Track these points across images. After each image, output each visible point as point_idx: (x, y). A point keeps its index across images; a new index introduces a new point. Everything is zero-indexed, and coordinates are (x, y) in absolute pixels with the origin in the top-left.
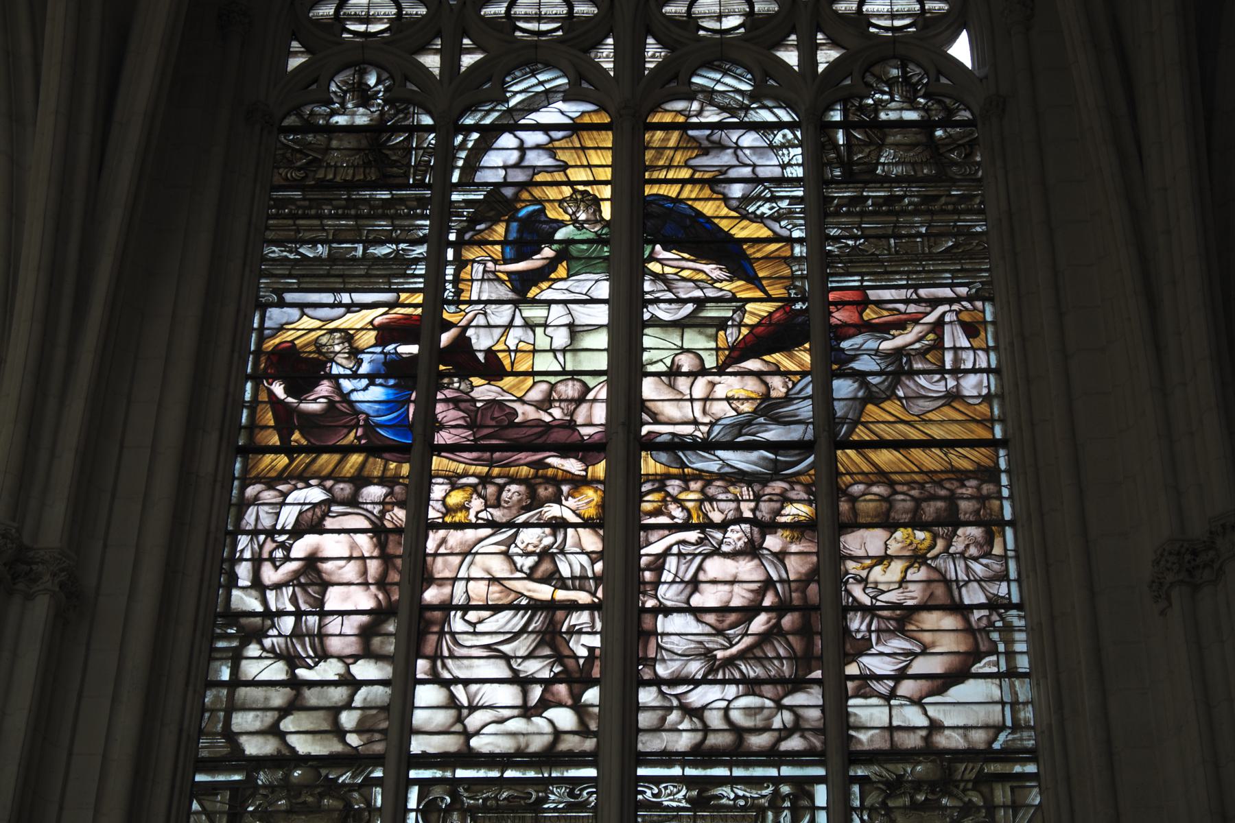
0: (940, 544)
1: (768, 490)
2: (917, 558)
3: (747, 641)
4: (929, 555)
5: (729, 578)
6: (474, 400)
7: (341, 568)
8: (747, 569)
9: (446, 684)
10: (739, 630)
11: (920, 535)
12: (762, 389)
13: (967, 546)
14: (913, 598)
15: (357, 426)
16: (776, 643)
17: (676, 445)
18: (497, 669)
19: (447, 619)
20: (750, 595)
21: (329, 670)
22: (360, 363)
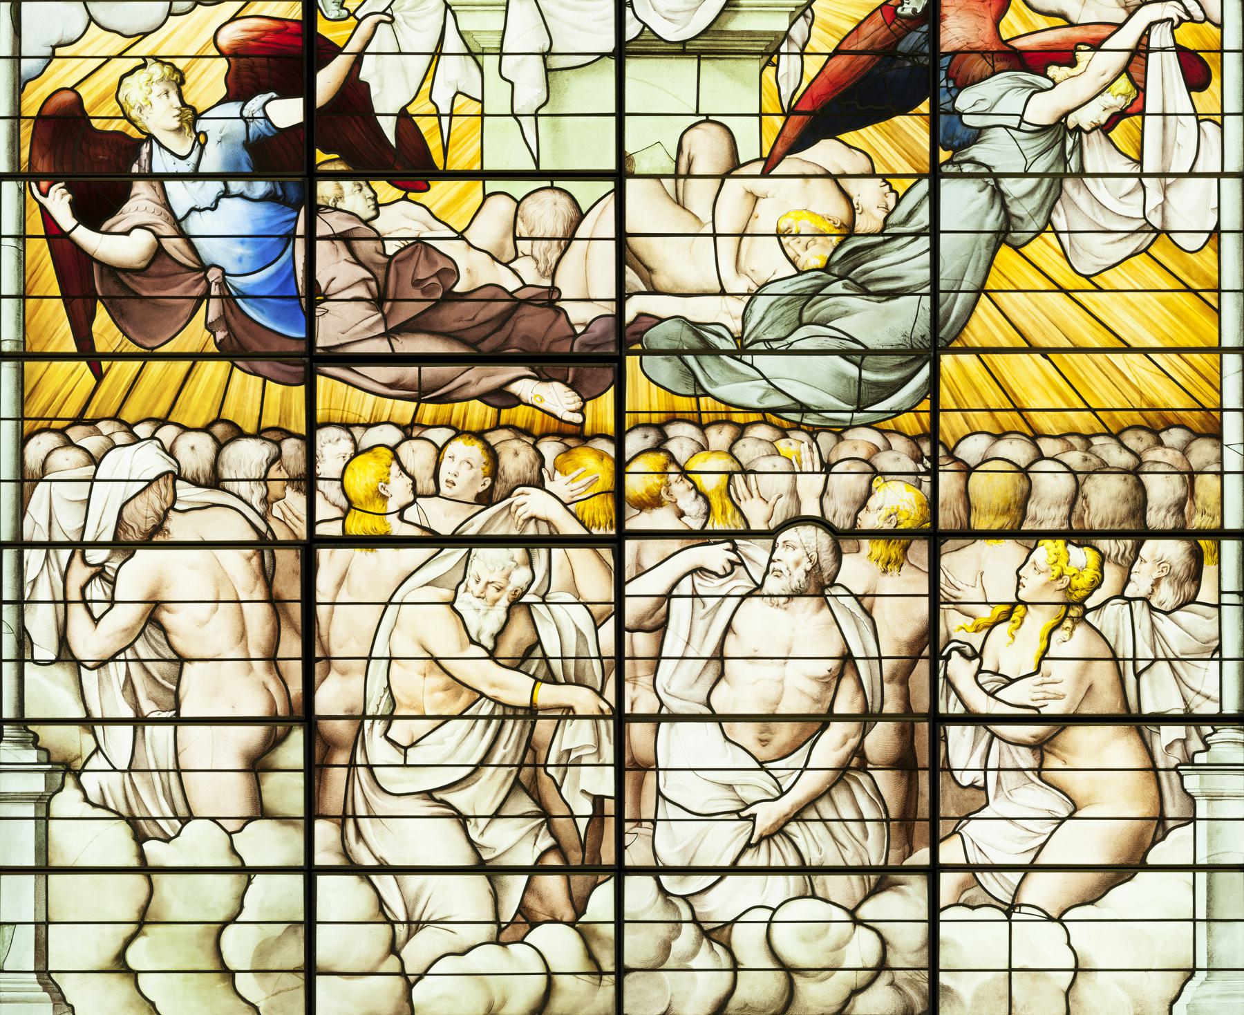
0: (1112, 574)
1: (845, 450)
2: (1074, 608)
3: (811, 783)
4: (1090, 603)
5: (783, 650)
6: (380, 238)
7: (203, 624)
8: (809, 631)
10: (797, 760)
11: (1082, 557)
12: (839, 211)
13: (1157, 582)
14: (1058, 697)
15: (207, 295)
16: (854, 786)
17: (701, 343)
18: (439, 842)
20: (815, 689)
21: (200, 845)
22: (201, 142)
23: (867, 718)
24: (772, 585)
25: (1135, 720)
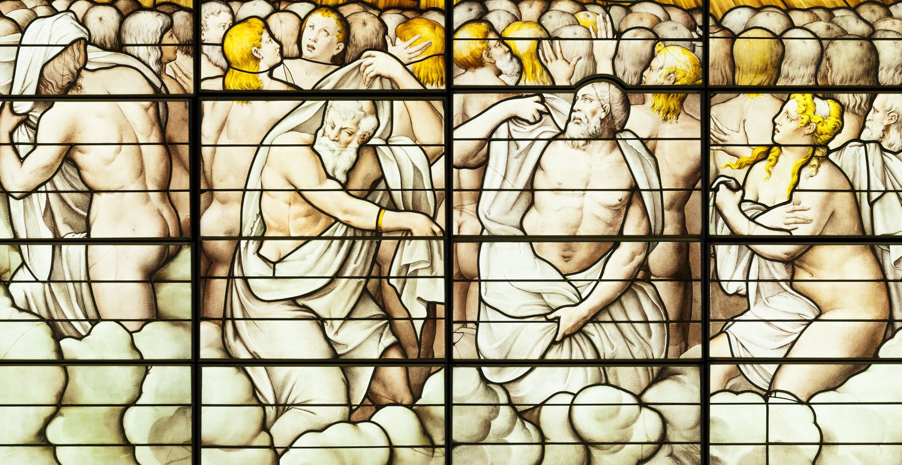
0: (850, 121)
1: (633, 21)
2: (819, 149)
3: (605, 291)
4: (832, 145)
5: (582, 184)
7: (109, 162)
8: (603, 167)
9: (240, 364)
10: (593, 273)
11: (826, 108)
13: (887, 128)
14: (806, 222)
16: (640, 294)
18: (304, 340)
19: (236, 255)
20: (608, 215)
21: (106, 341)
23: (650, 239)
24: (574, 130)
25: (870, 241)
